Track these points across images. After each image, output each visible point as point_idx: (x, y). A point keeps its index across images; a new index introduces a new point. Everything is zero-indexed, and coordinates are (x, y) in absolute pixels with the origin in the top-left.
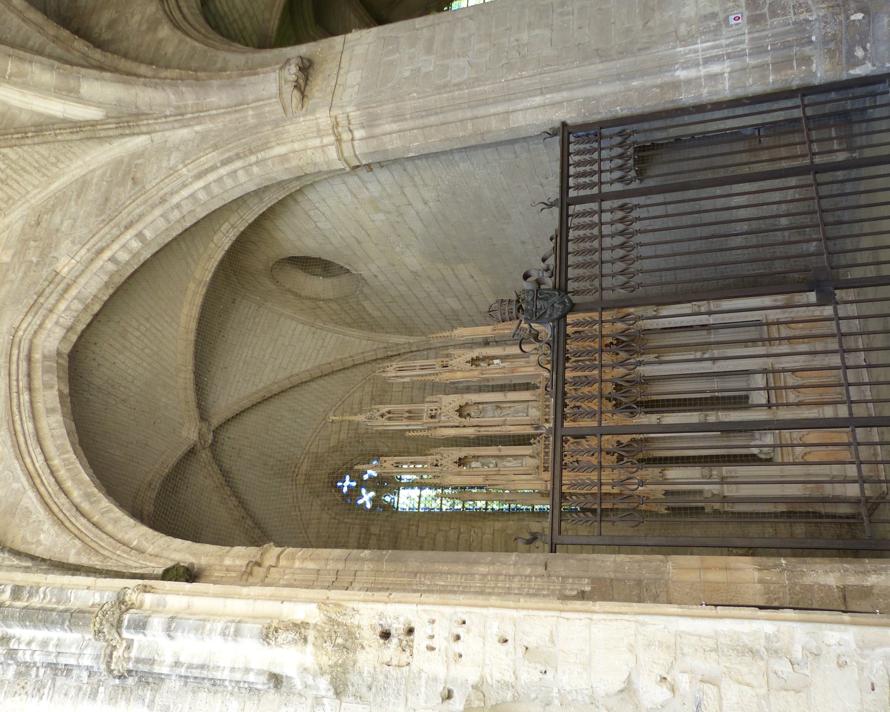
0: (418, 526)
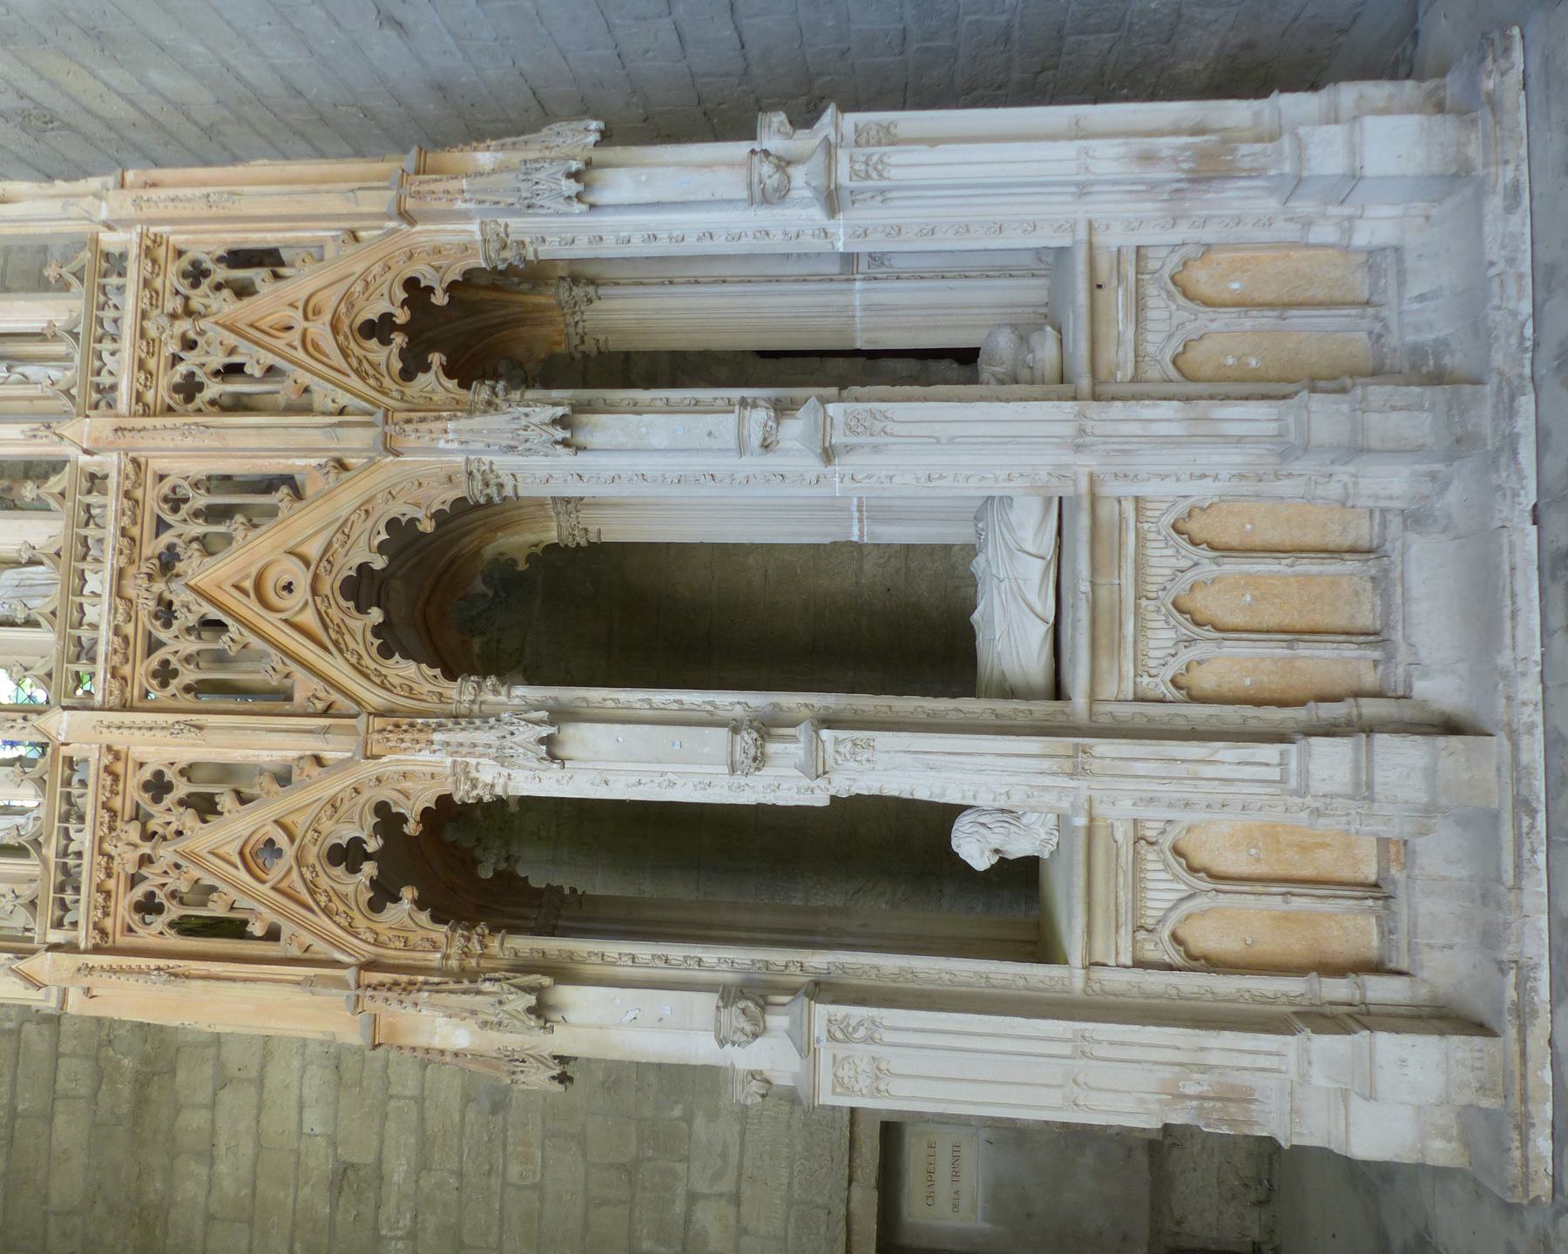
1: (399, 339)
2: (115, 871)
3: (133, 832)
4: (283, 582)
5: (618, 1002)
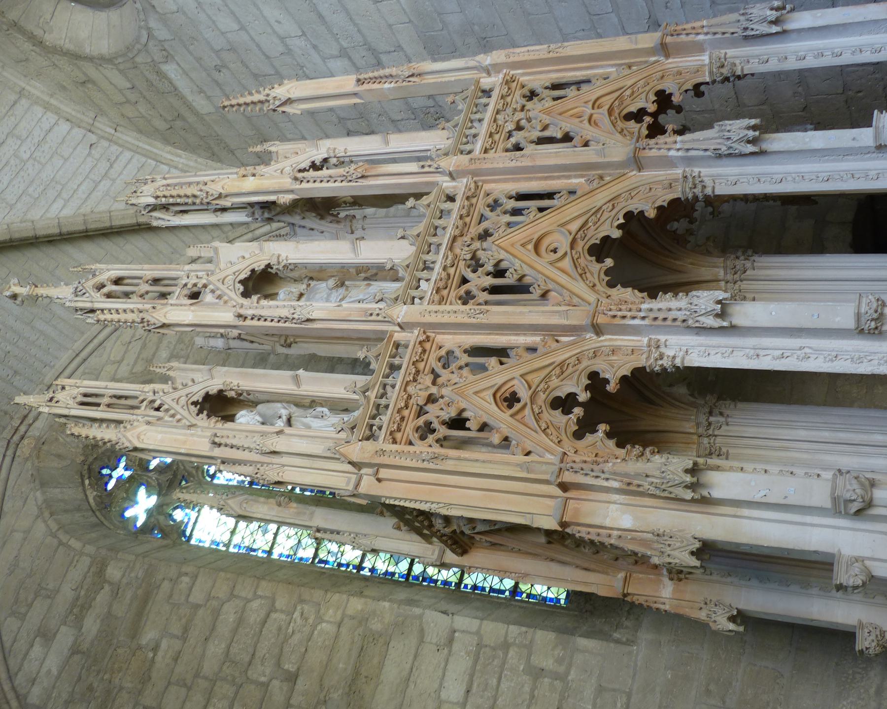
0: (195, 577)
1: (648, 119)
2: (410, 405)
3: (428, 380)
4: (551, 247)
5: (753, 483)
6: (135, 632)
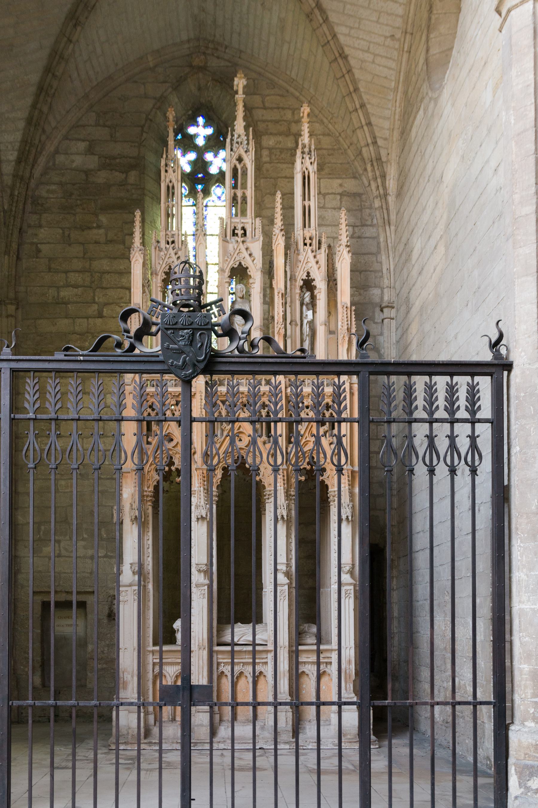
6: (106, 208)
